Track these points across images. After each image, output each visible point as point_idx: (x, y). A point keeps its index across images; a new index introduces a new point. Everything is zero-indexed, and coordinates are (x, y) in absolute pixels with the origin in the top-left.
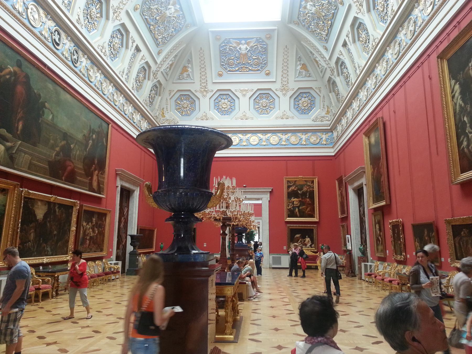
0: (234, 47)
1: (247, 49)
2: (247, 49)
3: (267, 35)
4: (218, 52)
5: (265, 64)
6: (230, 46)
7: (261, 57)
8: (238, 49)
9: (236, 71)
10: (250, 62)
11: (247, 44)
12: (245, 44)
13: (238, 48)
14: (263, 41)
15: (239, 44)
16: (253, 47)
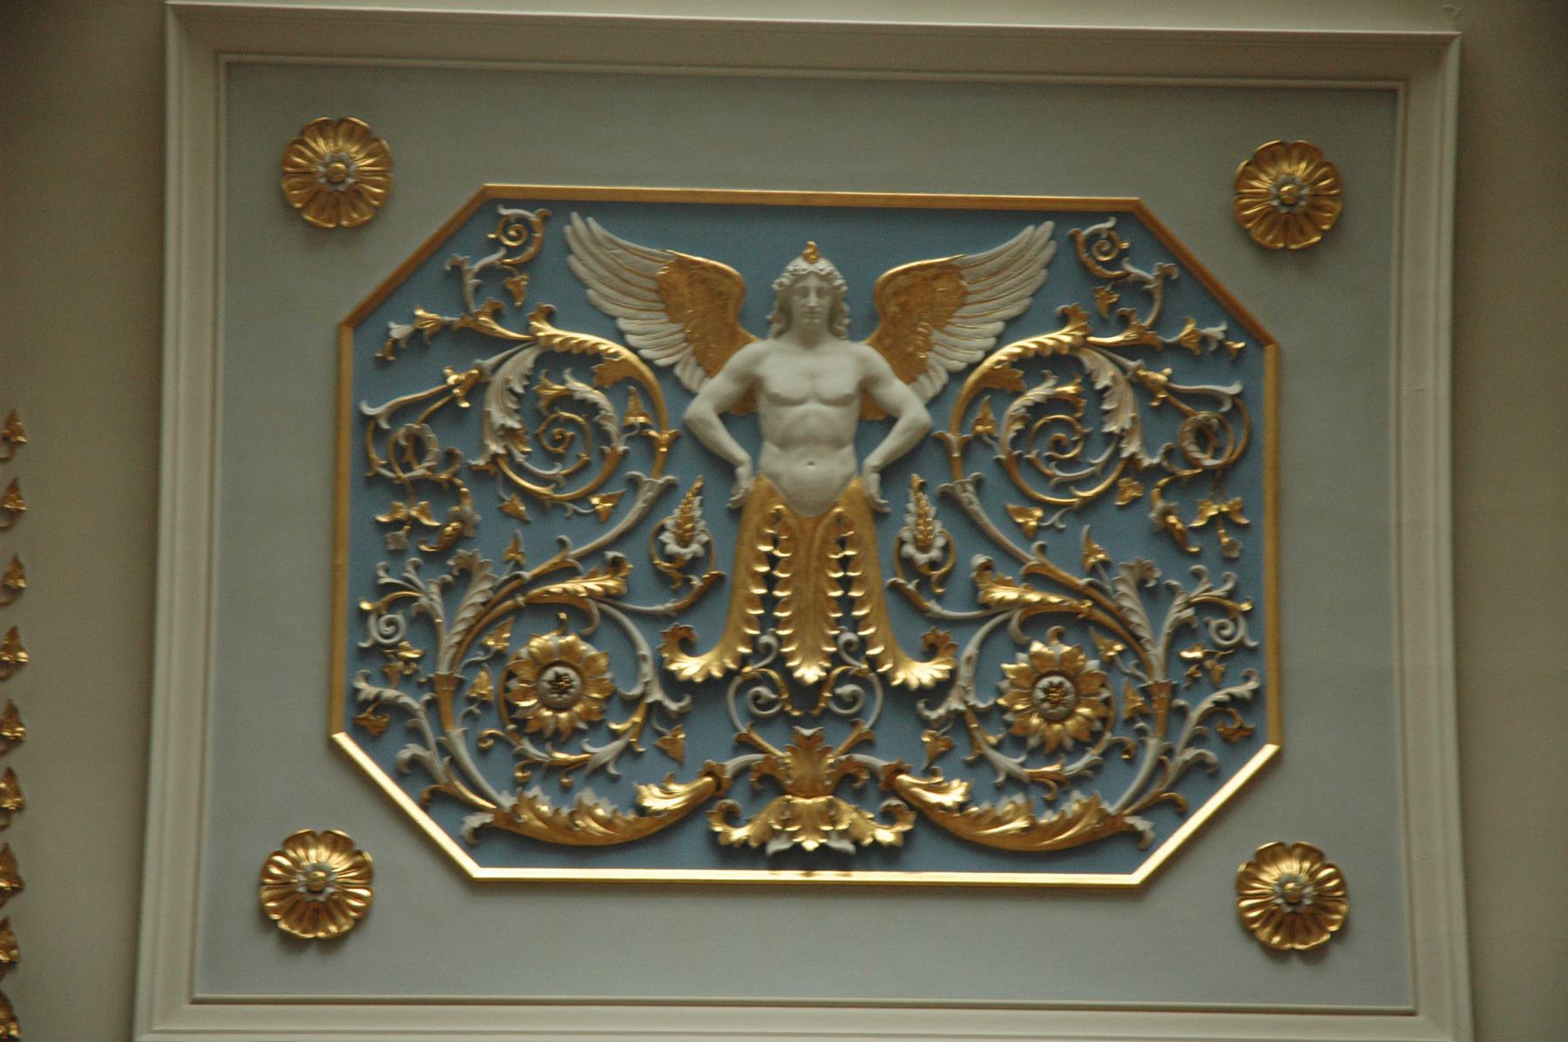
0: (623, 383)
1: (872, 416)
2: (872, 416)
3: (1261, 161)
4: (304, 471)
5: (1236, 726)
6: (555, 359)
7: (1154, 596)
8: (703, 408)
9: (655, 836)
10: (922, 673)
11: (897, 322)
12: (838, 321)
13: (710, 394)
14: (1192, 284)
15: (719, 317)
16: (999, 387)
